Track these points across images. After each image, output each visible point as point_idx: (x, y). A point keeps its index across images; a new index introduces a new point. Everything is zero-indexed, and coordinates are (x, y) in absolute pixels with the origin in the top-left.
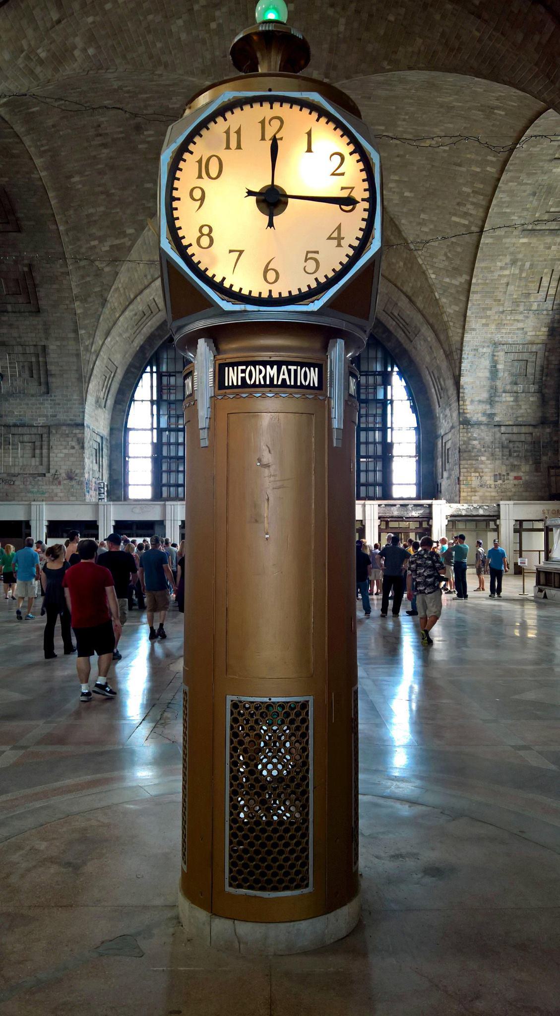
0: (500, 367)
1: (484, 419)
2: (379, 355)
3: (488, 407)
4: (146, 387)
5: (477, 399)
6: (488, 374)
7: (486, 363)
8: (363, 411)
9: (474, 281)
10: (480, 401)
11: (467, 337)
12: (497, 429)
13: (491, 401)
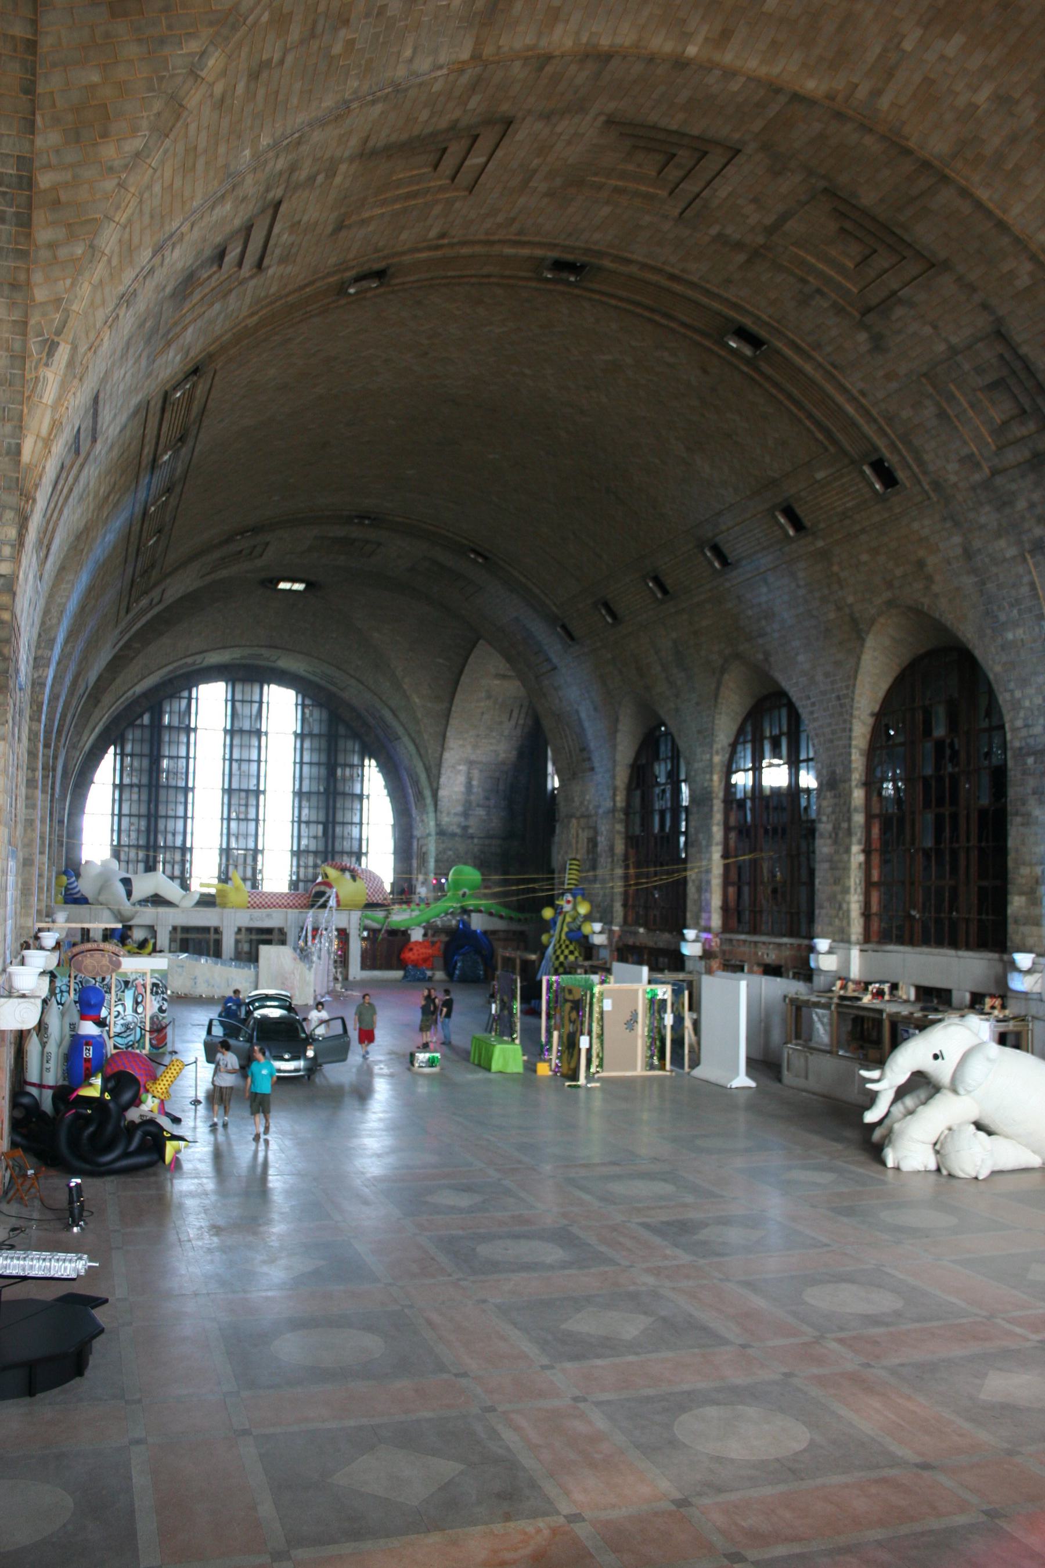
0: (475, 783)
1: (458, 831)
2: (357, 748)
3: (462, 819)
4: (107, 770)
5: (453, 811)
6: (463, 789)
7: (461, 779)
8: (338, 805)
9: (453, 709)
10: (456, 814)
11: (447, 755)
12: (470, 841)
13: (466, 815)
